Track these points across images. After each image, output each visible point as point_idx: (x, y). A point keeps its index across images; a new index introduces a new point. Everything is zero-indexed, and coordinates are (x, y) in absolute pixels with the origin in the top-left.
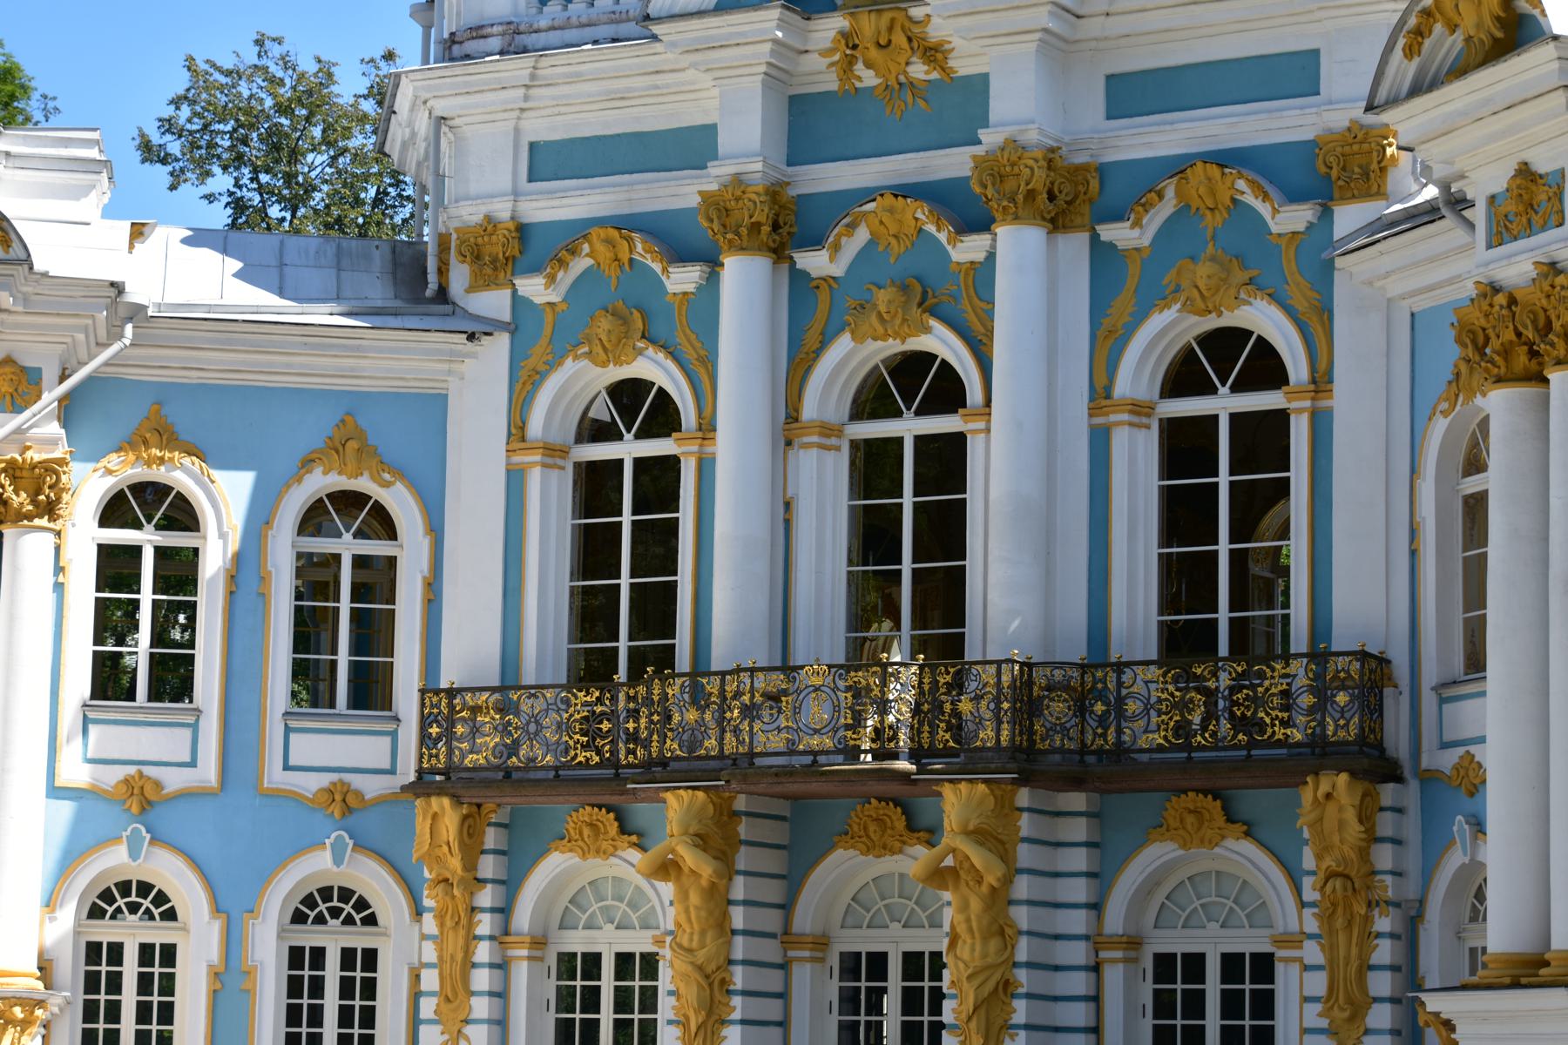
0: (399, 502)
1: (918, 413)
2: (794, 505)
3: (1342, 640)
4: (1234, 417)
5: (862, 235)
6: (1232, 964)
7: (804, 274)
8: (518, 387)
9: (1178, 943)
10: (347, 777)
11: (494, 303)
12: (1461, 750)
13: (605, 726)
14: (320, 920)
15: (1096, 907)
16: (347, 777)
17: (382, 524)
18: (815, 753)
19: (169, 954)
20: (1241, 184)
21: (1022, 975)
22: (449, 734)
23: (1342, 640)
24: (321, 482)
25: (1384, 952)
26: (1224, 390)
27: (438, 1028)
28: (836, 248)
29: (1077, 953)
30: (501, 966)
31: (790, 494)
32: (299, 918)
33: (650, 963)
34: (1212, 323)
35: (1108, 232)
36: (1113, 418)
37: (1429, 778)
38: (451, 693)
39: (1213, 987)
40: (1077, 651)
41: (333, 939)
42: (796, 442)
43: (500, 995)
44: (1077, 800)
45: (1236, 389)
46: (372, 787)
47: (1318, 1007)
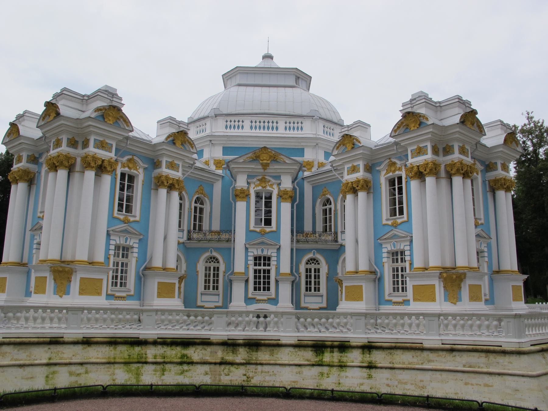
14: (210, 262)
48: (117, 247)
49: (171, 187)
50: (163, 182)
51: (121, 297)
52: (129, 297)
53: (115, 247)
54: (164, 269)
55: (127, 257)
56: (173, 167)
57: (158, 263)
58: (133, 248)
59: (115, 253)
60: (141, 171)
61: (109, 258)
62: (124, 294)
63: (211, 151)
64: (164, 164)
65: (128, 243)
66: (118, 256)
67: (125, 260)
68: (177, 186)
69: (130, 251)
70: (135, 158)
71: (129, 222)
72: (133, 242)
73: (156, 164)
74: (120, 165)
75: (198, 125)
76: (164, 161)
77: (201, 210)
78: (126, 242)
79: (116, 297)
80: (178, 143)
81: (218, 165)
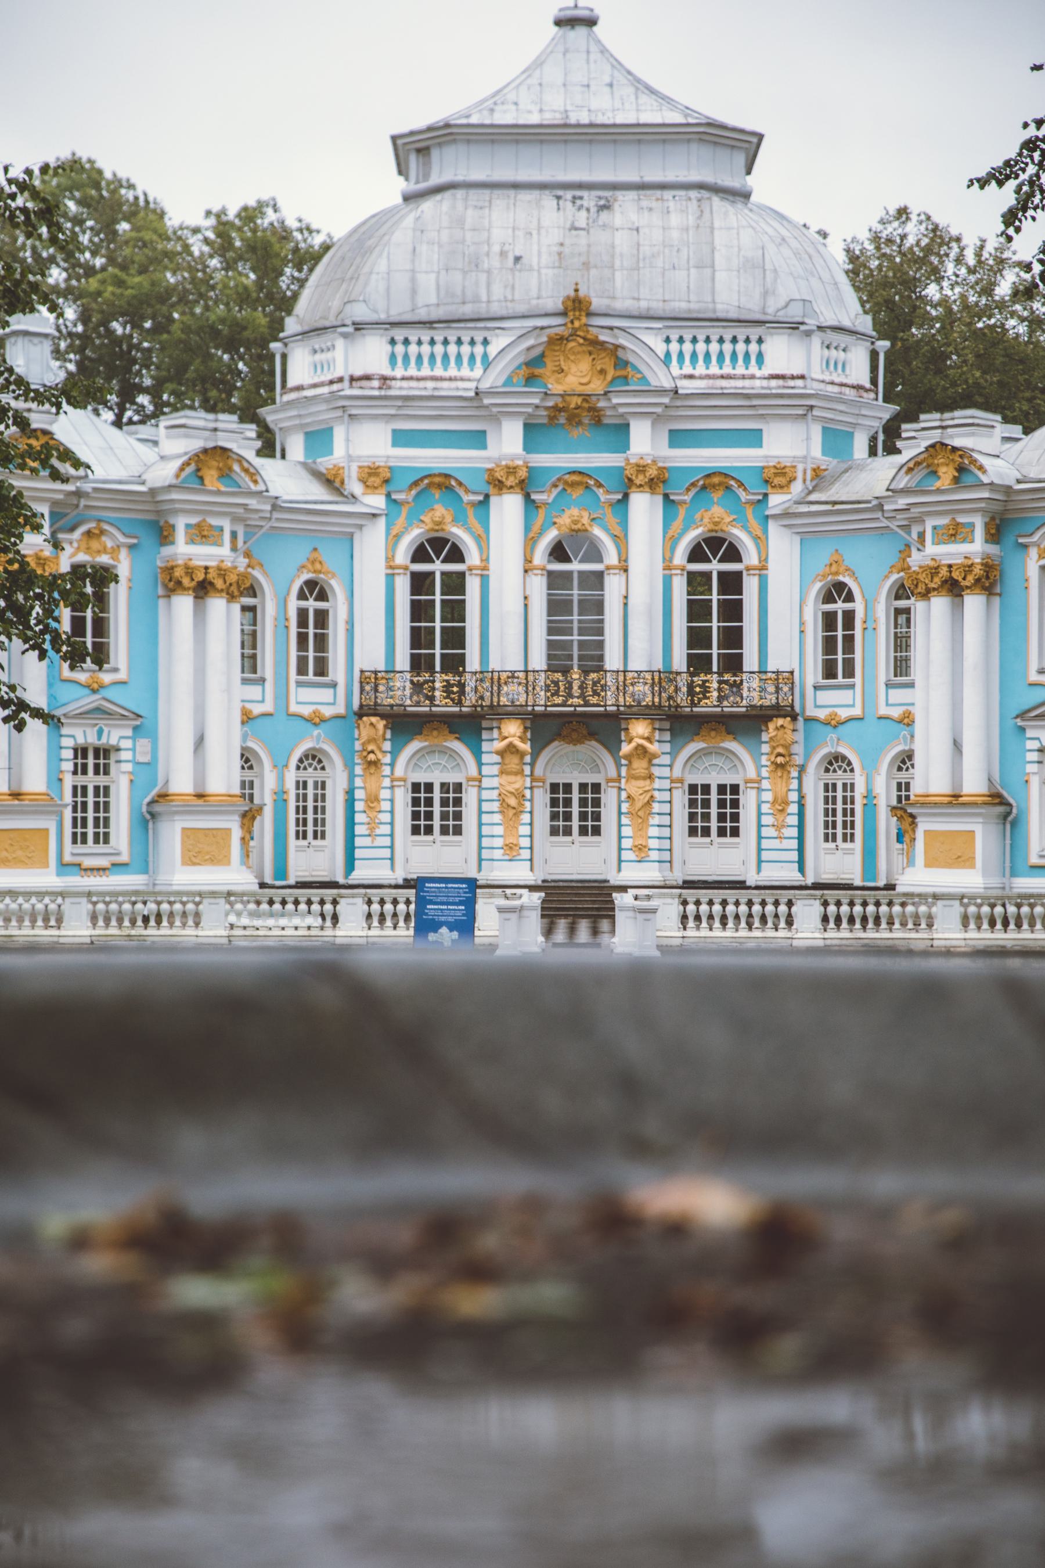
0: (337, 587)
1: (580, 562)
2: (530, 599)
3: (771, 666)
4: (721, 574)
5: (560, 488)
6: (722, 789)
7: (533, 501)
8: (391, 537)
9: (698, 779)
10: (319, 707)
11: (377, 501)
12: (830, 710)
13: (455, 689)
15: (671, 766)
16: (319, 707)
17: (322, 596)
18: (575, 706)
19: (252, 783)
20: (732, 483)
21: (656, 794)
22: (376, 690)
23: (771, 666)
24: (306, 576)
25: (794, 784)
26: (715, 562)
27: (364, 815)
28: (550, 491)
29: (666, 784)
30: (392, 787)
31: (527, 593)
32: (298, 768)
33: (458, 788)
34: (714, 534)
35: (672, 497)
36: (674, 572)
37: (808, 720)
38: (376, 672)
39: (714, 797)
40: (658, 665)
41: (311, 775)
42: (530, 573)
43: (392, 801)
44: (667, 725)
45: (720, 561)
46: (327, 712)
47: (768, 805)
48: (80, 752)
49: (203, 589)
50: (179, 583)
51: (98, 869)
52: (119, 867)
53: (76, 750)
54: (200, 796)
55: (106, 773)
56: (204, 536)
57: (182, 784)
58: (118, 749)
59: (76, 765)
60: (123, 554)
61: (60, 780)
62: (104, 862)
63: (347, 440)
64: (180, 535)
65: (104, 740)
66: (85, 772)
67: (101, 780)
68: (219, 584)
69: (113, 757)
70: (106, 527)
71: (102, 686)
72: (115, 735)
73: (164, 535)
74: (69, 550)
75: (317, 347)
76: (181, 524)
77: (322, 617)
78: (99, 738)
79: (86, 870)
80: (211, 477)
81: (375, 481)
